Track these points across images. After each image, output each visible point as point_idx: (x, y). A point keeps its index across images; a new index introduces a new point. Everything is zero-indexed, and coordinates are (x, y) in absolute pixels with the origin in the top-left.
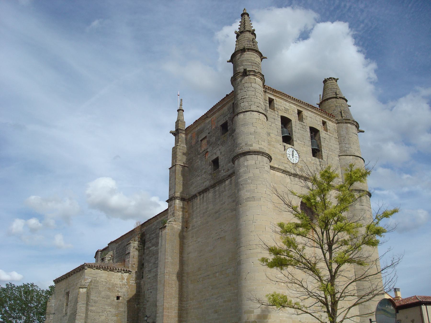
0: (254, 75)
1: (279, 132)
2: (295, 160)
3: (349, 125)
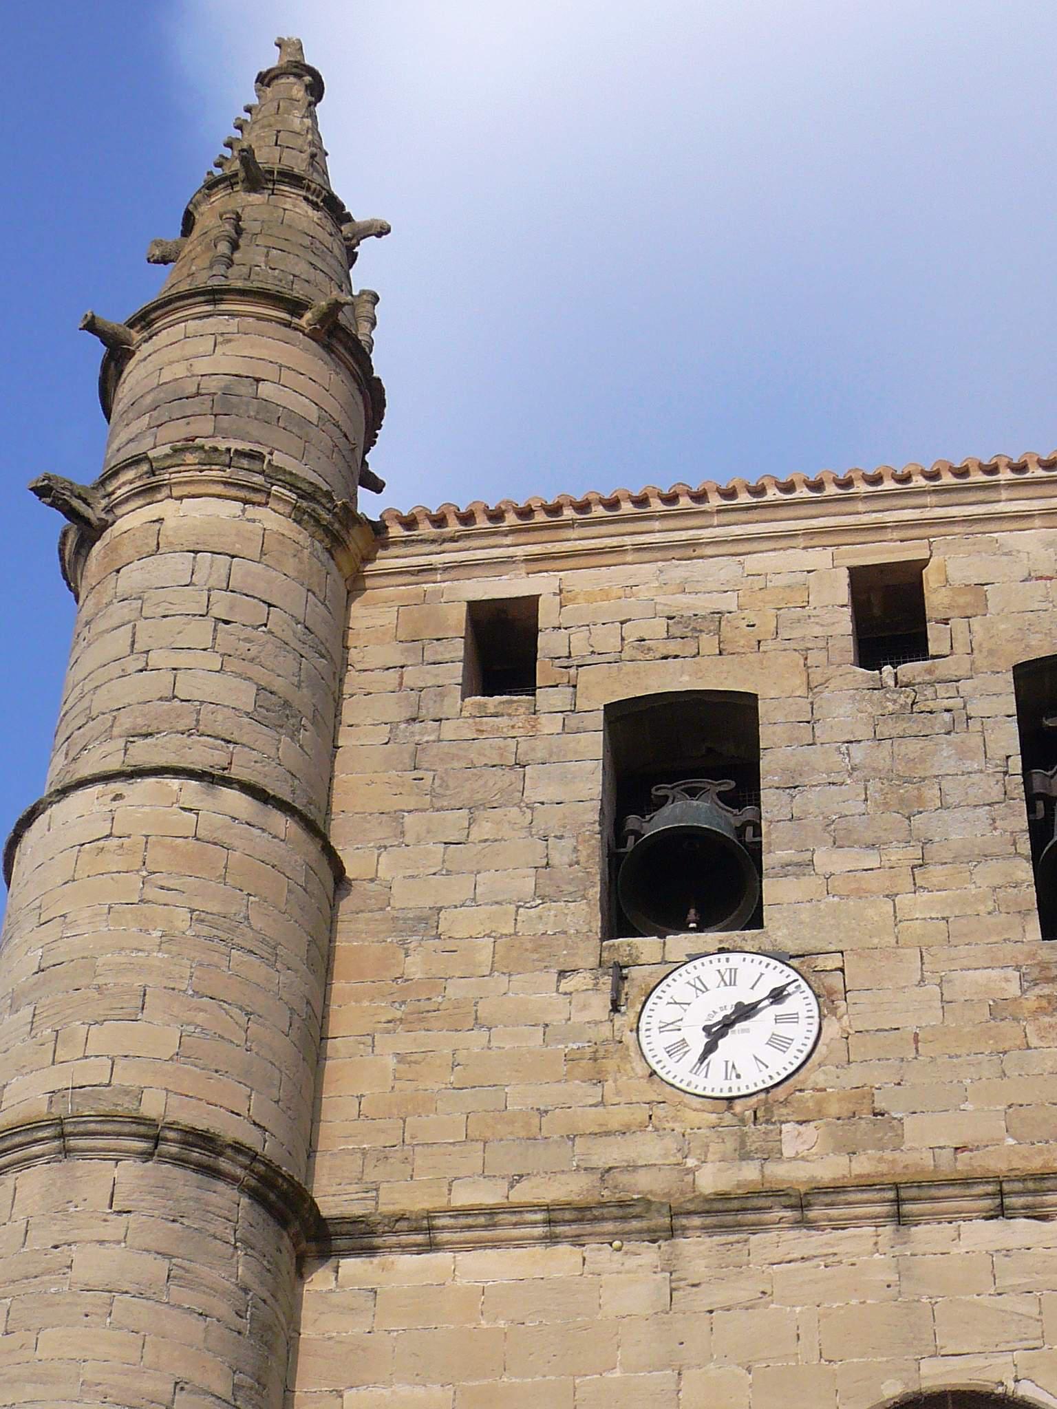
0: (149, 491)
1: (560, 858)
2: (753, 1059)
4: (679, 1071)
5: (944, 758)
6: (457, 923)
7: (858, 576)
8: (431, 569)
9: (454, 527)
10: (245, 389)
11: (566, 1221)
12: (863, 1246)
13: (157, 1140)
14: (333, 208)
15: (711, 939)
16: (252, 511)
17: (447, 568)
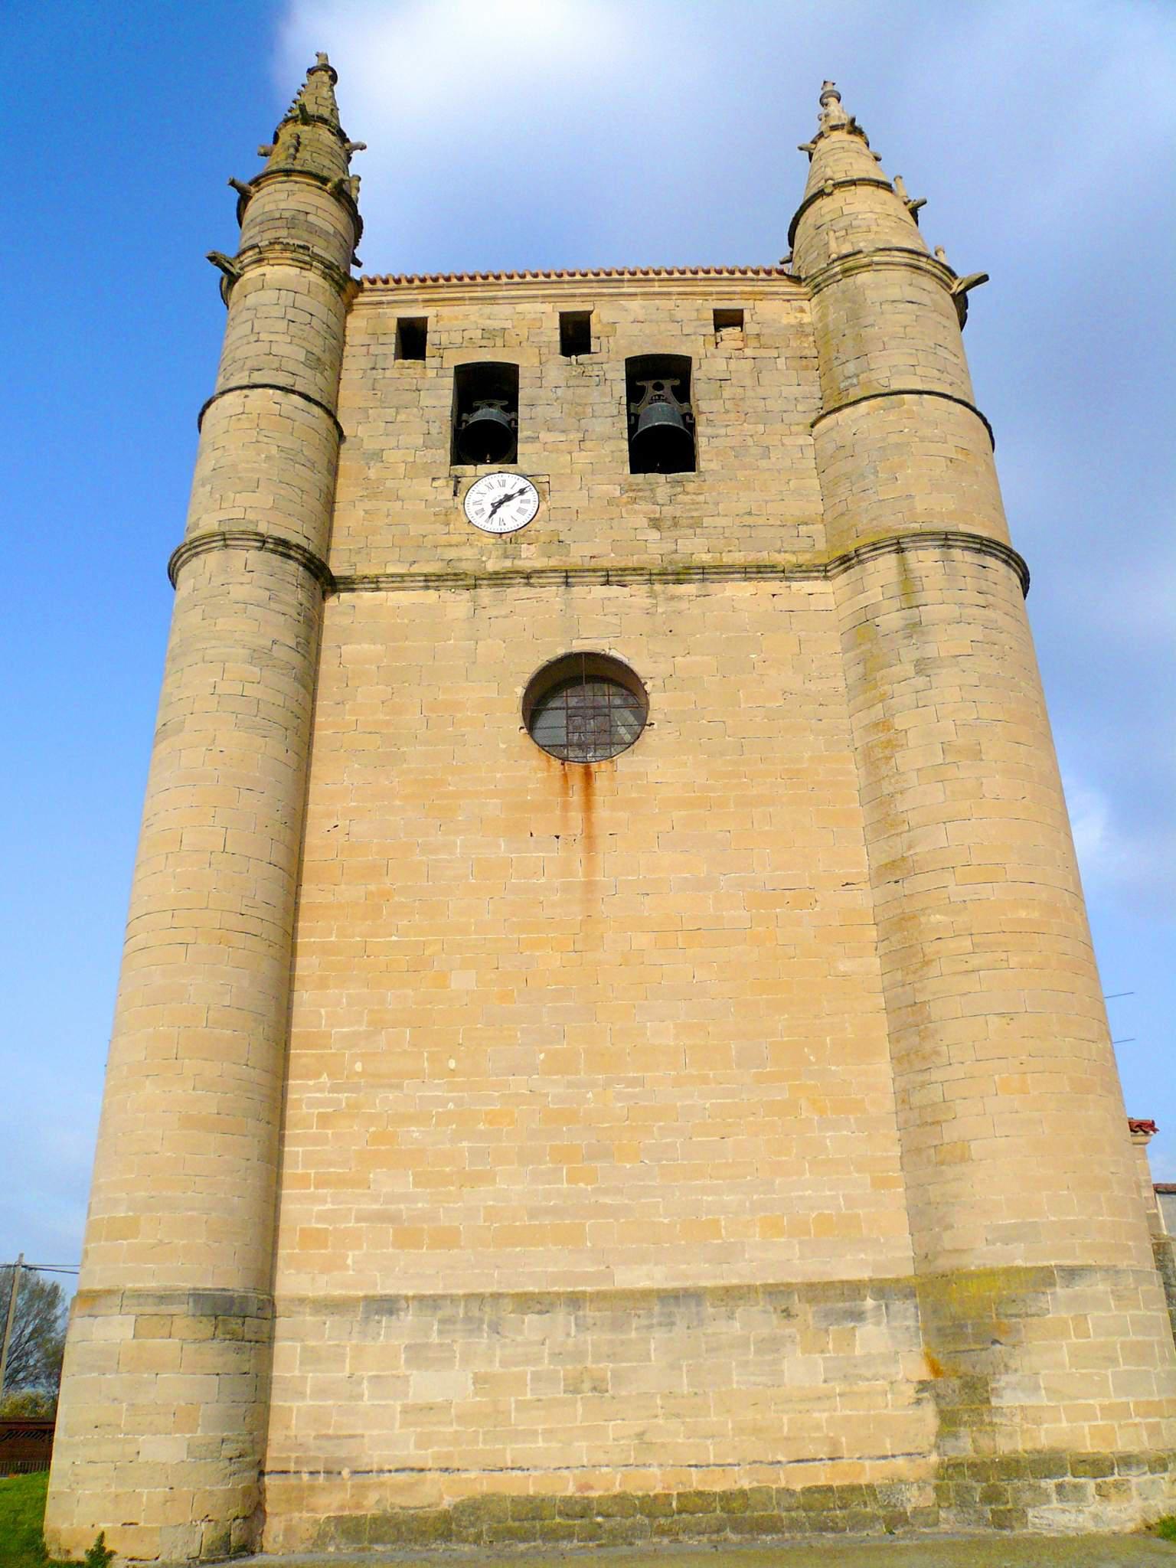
1: (434, 431)
2: (511, 517)
3: (864, 277)
4: (480, 521)
5: (595, 395)
6: (391, 456)
7: (562, 315)
8: (381, 303)
9: (392, 285)
10: (302, 217)
11: (431, 581)
12: (552, 594)
13: (264, 542)
14: (341, 135)
15: (496, 467)
16: (305, 273)
17: (389, 303)
